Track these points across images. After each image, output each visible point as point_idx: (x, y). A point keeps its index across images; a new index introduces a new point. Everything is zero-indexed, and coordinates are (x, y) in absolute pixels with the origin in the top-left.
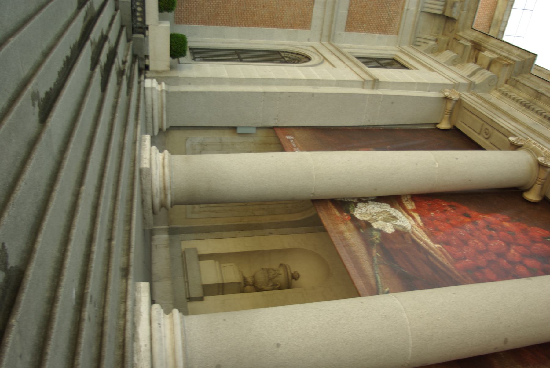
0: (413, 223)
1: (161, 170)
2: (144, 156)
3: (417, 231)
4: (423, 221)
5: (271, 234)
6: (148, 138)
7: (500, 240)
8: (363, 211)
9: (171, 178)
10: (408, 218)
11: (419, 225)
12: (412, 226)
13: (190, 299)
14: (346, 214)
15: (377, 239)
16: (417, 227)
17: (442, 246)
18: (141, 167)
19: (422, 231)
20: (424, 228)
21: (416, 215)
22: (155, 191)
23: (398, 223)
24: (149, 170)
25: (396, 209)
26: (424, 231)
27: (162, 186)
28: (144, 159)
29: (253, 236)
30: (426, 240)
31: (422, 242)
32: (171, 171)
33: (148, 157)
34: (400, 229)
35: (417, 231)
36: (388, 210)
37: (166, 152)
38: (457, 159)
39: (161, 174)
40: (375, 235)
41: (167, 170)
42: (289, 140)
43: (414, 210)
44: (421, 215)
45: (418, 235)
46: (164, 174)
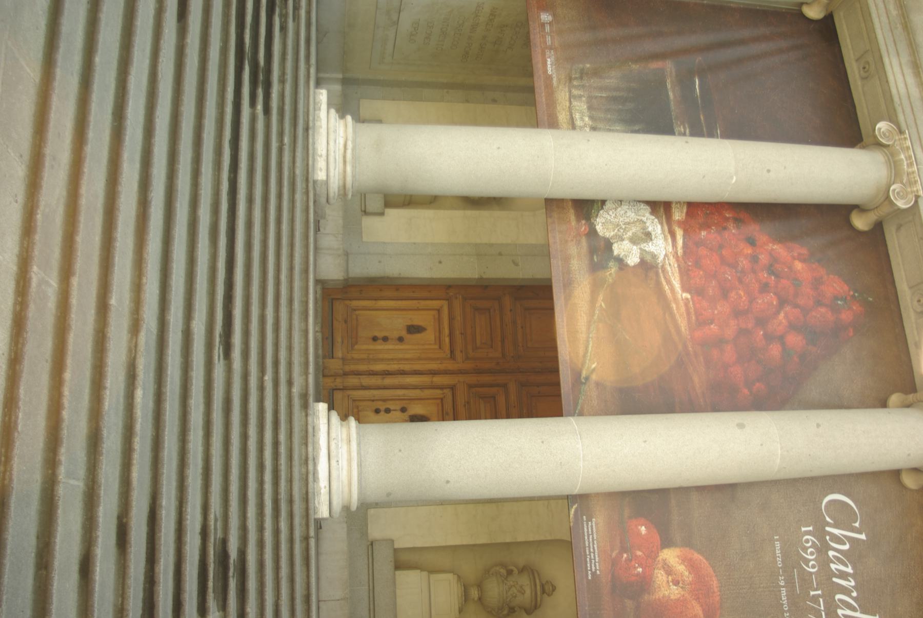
0: (670, 249)
1: (341, 165)
2: (319, 152)
3: (670, 265)
4: (685, 246)
5: (494, 101)
6: (323, 96)
7: (775, 294)
8: (609, 218)
9: (354, 176)
10: (666, 239)
11: (677, 254)
12: (666, 255)
13: (365, 213)
14: (583, 222)
15: (610, 274)
16: (671, 257)
17: (691, 296)
18: (316, 178)
19: (676, 265)
20: (681, 259)
21: (679, 234)
22: (331, 195)
23: (650, 247)
24: (327, 183)
25: (657, 217)
26: (679, 266)
27: (341, 183)
28: (319, 158)
29: (467, 101)
30: (674, 282)
31: (668, 286)
32: (354, 167)
33: (324, 153)
34: (648, 258)
35: (670, 265)
36: (644, 219)
37: (349, 118)
38: (769, 171)
39: (341, 171)
40: (611, 268)
41: (349, 169)
42: (543, 25)
43: (680, 223)
44: (686, 232)
45: (668, 273)
46: (345, 171)
